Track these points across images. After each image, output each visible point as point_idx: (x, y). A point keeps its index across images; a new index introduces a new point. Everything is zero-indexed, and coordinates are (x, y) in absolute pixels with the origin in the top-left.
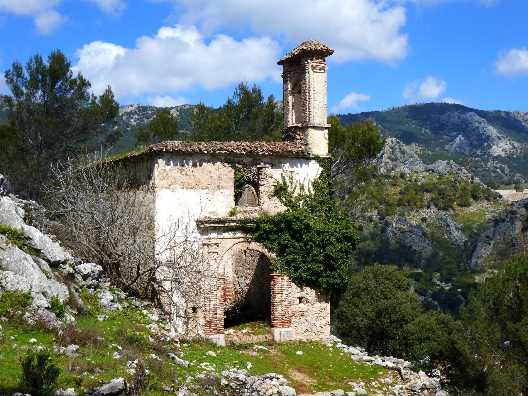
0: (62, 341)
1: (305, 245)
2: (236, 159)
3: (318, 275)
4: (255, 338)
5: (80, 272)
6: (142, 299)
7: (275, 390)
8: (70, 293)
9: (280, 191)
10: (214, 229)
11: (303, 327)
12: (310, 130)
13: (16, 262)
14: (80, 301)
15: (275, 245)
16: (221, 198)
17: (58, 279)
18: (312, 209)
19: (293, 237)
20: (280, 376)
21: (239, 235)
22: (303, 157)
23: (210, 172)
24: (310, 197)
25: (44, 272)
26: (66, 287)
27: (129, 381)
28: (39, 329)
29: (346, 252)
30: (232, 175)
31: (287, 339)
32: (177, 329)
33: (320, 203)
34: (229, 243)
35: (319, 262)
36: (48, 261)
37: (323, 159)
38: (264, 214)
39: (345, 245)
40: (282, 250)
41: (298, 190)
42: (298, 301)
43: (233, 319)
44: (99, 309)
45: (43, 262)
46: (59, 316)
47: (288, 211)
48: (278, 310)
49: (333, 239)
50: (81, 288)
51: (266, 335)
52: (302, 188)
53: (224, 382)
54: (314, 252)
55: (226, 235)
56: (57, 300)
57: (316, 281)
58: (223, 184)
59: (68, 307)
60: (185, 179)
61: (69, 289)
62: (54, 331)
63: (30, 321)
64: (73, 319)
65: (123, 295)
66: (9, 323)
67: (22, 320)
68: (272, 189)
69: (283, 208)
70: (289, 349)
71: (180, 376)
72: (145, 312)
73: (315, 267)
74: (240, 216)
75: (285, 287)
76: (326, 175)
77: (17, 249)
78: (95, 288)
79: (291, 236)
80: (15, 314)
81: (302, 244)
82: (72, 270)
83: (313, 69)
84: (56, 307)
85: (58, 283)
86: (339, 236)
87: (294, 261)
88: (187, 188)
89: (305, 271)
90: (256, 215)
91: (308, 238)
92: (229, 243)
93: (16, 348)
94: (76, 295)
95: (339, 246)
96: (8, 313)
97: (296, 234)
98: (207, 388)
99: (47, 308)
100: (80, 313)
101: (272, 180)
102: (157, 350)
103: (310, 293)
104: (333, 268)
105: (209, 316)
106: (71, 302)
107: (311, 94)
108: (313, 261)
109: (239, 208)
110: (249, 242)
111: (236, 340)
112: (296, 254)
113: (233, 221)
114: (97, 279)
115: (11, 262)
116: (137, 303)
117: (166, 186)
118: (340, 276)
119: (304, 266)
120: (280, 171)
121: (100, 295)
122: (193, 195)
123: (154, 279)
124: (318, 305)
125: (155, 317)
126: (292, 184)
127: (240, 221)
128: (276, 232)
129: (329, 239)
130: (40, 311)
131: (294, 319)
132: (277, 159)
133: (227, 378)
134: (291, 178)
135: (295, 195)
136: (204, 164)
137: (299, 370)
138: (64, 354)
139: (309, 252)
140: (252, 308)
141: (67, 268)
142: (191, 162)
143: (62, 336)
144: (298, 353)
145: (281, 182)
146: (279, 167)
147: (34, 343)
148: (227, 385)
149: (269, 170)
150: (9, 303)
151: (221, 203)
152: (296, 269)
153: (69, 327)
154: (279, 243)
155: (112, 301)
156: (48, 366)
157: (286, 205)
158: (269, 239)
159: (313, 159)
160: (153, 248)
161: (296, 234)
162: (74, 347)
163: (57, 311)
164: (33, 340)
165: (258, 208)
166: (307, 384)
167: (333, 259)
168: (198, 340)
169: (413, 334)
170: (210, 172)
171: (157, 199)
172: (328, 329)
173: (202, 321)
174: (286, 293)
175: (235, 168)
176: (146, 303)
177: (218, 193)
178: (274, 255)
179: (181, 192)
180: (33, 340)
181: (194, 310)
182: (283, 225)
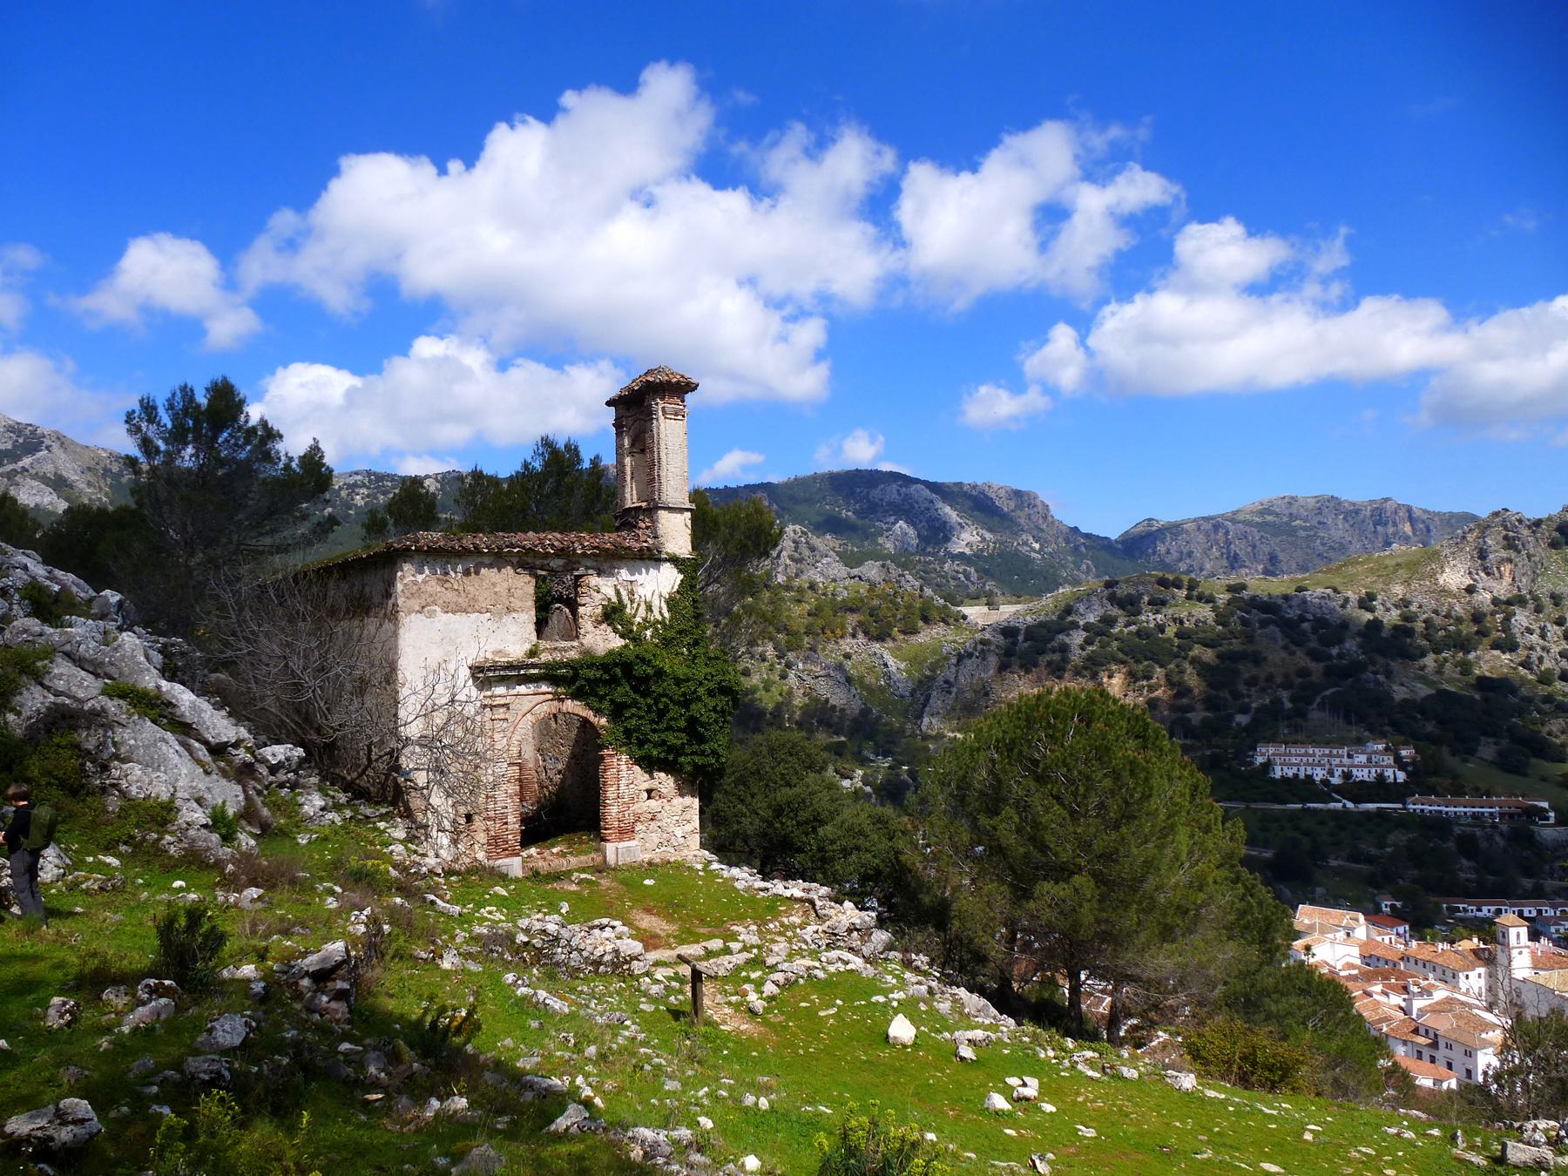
0: (232, 884)
1: (656, 703)
2: (538, 562)
3: (678, 751)
4: (574, 861)
5: (264, 761)
6: (377, 803)
7: (609, 948)
8: (247, 797)
9: (612, 614)
10: (502, 680)
12: (662, 513)
13: (146, 747)
14: (265, 812)
15: (606, 705)
16: (513, 628)
17: (224, 774)
18: (667, 642)
19: (635, 689)
20: (617, 923)
21: (544, 688)
22: (652, 557)
23: (494, 584)
24: (663, 623)
25: (199, 762)
26: (240, 788)
27: (355, 946)
28: (191, 863)
29: (723, 711)
30: (531, 589)
31: (628, 860)
32: (439, 851)
33: (680, 632)
34: (527, 703)
35: (680, 730)
36: (206, 743)
37: (684, 560)
38: (587, 652)
39: (722, 701)
40: (617, 713)
41: (642, 612)
43: (536, 830)
44: (301, 823)
45: (197, 745)
46: (228, 838)
47: (626, 646)
48: (612, 812)
49: (701, 691)
50: (267, 787)
51: (593, 855)
52: (649, 608)
53: (521, 938)
54: (669, 715)
55: (522, 689)
56: (223, 812)
57: (675, 760)
58: (516, 603)
59: (243, 823)
60: (450, 596)
61: (245, 791)
62: (219, 865)
63: (172, 850)
64: (252, 842)
65: (343, 798)
66: (133, 855)
67: (158, 849)
68: (599, 610)
69: (617, 642)
70: (630, 876)
71: (445, 932)
72: (382, 825)
73: (673, 739)
74: (545, 657)
75: (624, 774)
76: (687, 586)
77: (149, 723)
78: (292, 788)
79: (632, 687)
80: (144, 840)
81: (650, 701)
82: (249, 758)
83: (664, 413)
84: (221, 824)
85: (224, 782)
86: (712, 685)
87: (637, 729)
88: (454, 612)
89: (656, 745)
90: (573, 655)
91: (660, 690)
92: (527, 703)
93: (148, 899)
94: (258, 800)
95: (711, 703)
96: (132, 837)
97: (641, 685)
98: (492, 951)
99: (205, 826)
100: (266, 832)
101: (600, 596)
102: (403, 890)
103: (665, 782)
104: (702, 740)
105: (494, 827)
106: (248, 814)
107: (663, 455)
108: (669, 728)
109: (543, 644)
110: (562, 700)
111: (541, 865)
112: (641, 718)
113: (534, 666)
114: (296, 773)
115: (137, 747)
116: (368, 811)
117: (417, 608)
118: (714, 752)
119: (655, 737)
120: (612, 581)
121: (301, 800)
122: (463, 624)
123: (397, 768)
124: (678, 801)
125: (400, 834)
126: (632, 602)
127: (546, 665)
128: (606, 683)
129: (695, 692)
130: (191, 832)
131: (639, 827)
132: (607, 561)
133: (527, 931)
134: (632, 593)
135: (638, 619)
136: (483, 571)
137: (648, 911)
138: (236, 905)
139: (662, 714)
140: (567, 810)
141: (242, 755)
142: (460, 568)
143: (232, 874)
144: (647, 882)
145: (614, 599)
146: (611, 575)
147: (181, 889)
148: (526, 944)
149: (594, 580)
150: (133, 819)
151: (513, 637)
152: (641, 743)
153: (246, 858)
154: (612, 701)
155: (322, 809)
156: (206, 927)
157: (622, 636)
158: (596, 695)
159: (666, 560)
160: (396, 715)
161: (641, 685)
162: (254, 892)
163: (224, 831)
164: (178, 884)
165: (575, 644)
166: (663, 934)
167: (702, 725)
168: (476, 869)
169: (833, 842)
170: (494, 584)
171: (401, 631)
172: (696, 840)
173: (481, 837)
174: (626, 783)
175: (537, 577)
176: (383, 811)
177: (507, 619)
178: (603, 721)
180: (178, 884)
181: (469, 818)
182: (618, 671)
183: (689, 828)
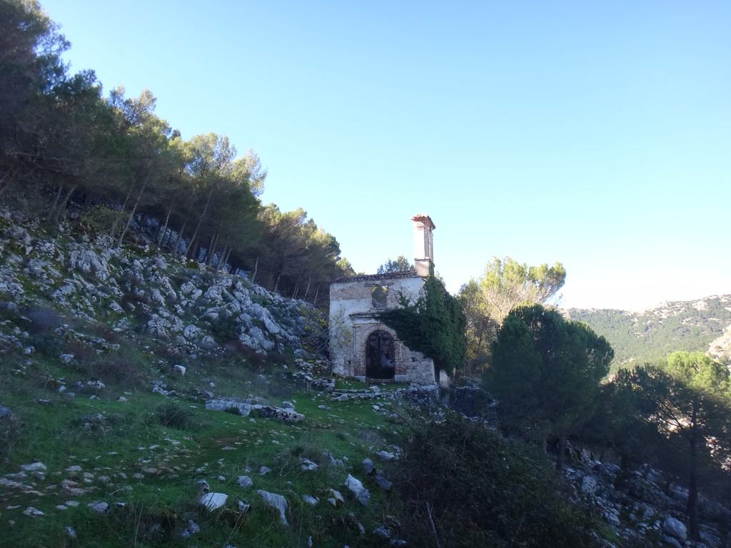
21: (373, 321)
42: (411, 360)
58: (365, 296)
75: (401, 351)
103: (419, 355)
122: (347, 303)
124: (425, 363)
157: (401, 304)
179: (342, 302)
183: (428, 373)
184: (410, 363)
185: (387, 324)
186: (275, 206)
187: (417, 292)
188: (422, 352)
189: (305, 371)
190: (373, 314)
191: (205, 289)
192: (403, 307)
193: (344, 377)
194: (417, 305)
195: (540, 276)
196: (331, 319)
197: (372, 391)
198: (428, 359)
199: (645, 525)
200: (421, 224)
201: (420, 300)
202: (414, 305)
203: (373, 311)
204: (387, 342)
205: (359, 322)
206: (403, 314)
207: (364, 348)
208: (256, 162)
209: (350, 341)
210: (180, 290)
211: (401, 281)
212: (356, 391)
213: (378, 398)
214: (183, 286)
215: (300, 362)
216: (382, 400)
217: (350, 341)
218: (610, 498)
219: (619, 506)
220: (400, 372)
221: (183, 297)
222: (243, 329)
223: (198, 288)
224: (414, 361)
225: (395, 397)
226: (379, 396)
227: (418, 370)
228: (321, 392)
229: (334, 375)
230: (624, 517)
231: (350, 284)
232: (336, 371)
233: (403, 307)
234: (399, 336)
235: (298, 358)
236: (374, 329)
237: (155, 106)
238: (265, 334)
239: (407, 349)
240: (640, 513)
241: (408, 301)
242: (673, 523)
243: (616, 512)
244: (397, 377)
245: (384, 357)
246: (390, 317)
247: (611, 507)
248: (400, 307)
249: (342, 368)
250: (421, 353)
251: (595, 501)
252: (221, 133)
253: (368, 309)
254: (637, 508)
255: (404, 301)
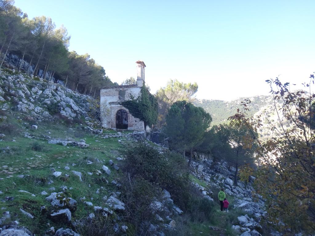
11: (136, 127)
21: (119, 105)
42: (135, 121)
60: (107, 94)
103: (138, 119)
122: (108, 98)
173: (110, 125)
179: (106, 97)
183: (141, 127)
184: (134, 123)
185: (125, 107)
186: (75, 52)
187: (137, 94)
188: (139, 118)
189: (90, 126)
190: (119, 102)
191: (43, 90)
192: (132, 100)
193: (107, 128)
194: (137, 99)
195: (188, 87)
196: (101, 104)
197: (118, 134)
198: (141, 121)
199: (219, 181)
200: (140, 65)
201: (139, 97)
202: (136, 99)
203: (119, 101)
204: (125, 114)
205: (113, 106)
206: (131, 102)
207: (115, 117)
208: (65, 31)
209: (109, 114)
210: (32, 91)
211: (131, 89)
212: (111, 134)
213: (121, 137)
214: (33, 89)
215: (87, 123)
216: (122, 138)
217: (109, 114)
218: (208, 172)
219: (210, 175)
220: (130, 126)
221: (33, 94)
222: (62, 108)
223: (40, 90)
224: (136, 122)
225: (127, 136)
226: (121, 136)
227: (136, 125)
228: (97, 135)
229: (103, 128)
230: (212, 179)
231: (109, 90)
232: (103, 126)
233: (132, 100)
234: (130, 112)
235: (87, 121)
236: (119, 109)
237: (14, 2)
238: (72, 111)
239: (133, 117)
240: (218, 177)
241: (134, 97)
242: (228, 180)
243: (209, 177)
244: (129, 128)
245: (124, 120)
246: (126, 104)
247: (208, 175)
248: (130, 100)
249: (106, 125)
250: (139, 119)
251: (202, 173)
252: (48, 16)
253: (117, 100)
254: (217, 176)
255: (132, 97)
